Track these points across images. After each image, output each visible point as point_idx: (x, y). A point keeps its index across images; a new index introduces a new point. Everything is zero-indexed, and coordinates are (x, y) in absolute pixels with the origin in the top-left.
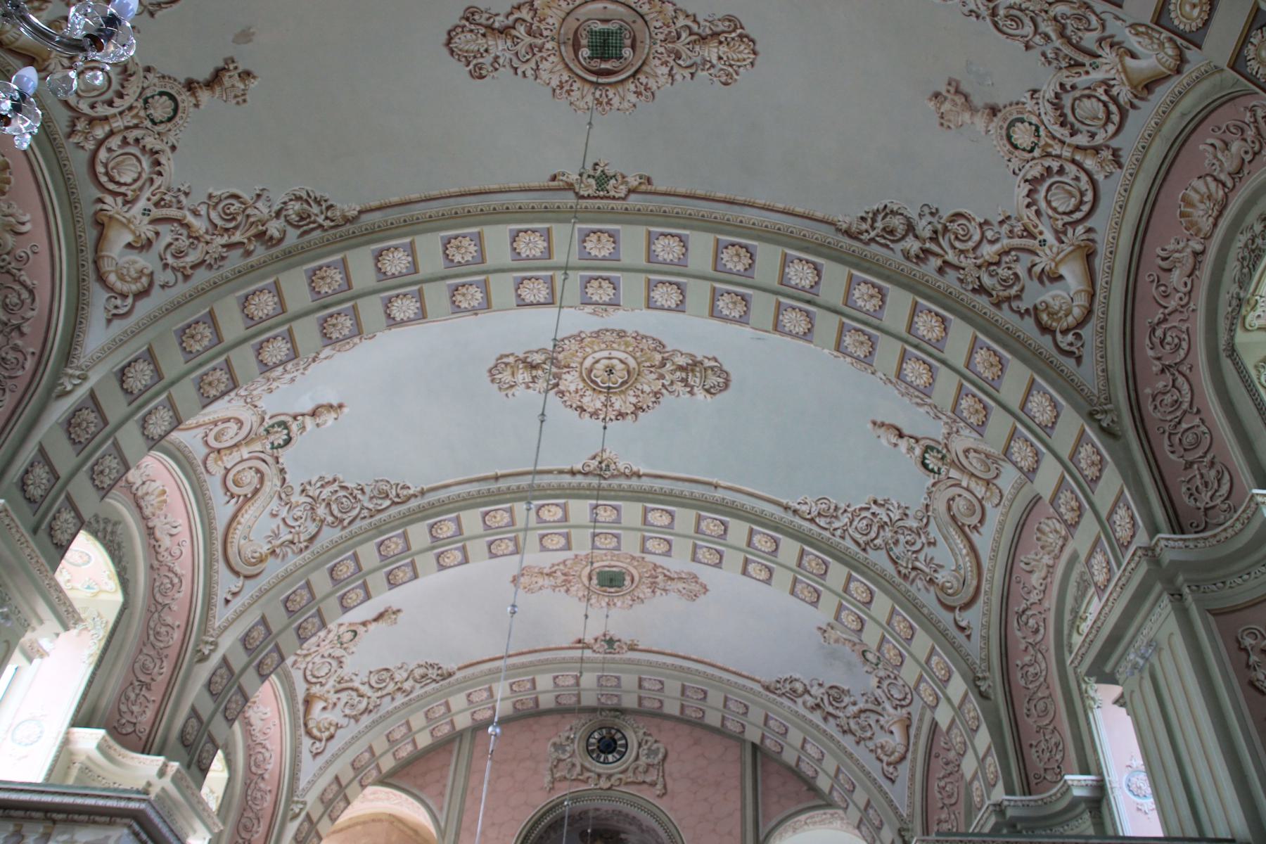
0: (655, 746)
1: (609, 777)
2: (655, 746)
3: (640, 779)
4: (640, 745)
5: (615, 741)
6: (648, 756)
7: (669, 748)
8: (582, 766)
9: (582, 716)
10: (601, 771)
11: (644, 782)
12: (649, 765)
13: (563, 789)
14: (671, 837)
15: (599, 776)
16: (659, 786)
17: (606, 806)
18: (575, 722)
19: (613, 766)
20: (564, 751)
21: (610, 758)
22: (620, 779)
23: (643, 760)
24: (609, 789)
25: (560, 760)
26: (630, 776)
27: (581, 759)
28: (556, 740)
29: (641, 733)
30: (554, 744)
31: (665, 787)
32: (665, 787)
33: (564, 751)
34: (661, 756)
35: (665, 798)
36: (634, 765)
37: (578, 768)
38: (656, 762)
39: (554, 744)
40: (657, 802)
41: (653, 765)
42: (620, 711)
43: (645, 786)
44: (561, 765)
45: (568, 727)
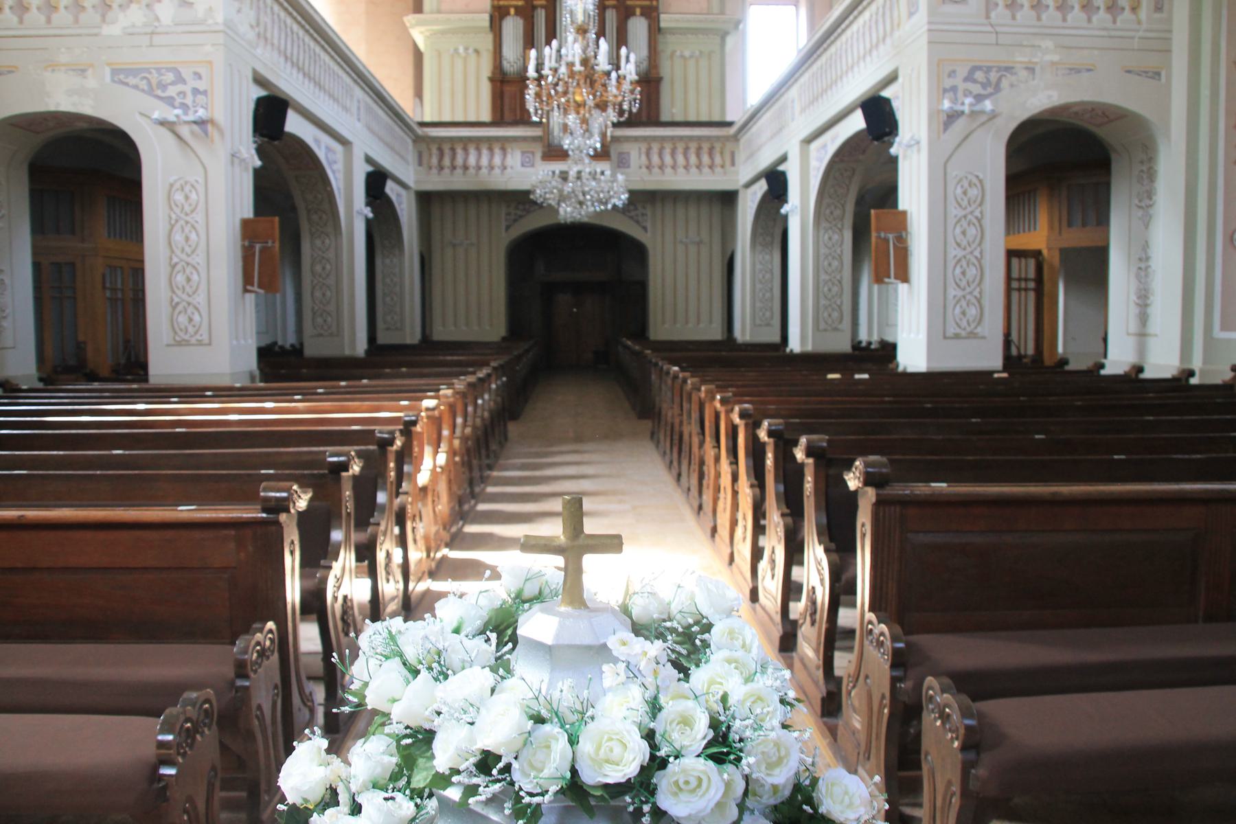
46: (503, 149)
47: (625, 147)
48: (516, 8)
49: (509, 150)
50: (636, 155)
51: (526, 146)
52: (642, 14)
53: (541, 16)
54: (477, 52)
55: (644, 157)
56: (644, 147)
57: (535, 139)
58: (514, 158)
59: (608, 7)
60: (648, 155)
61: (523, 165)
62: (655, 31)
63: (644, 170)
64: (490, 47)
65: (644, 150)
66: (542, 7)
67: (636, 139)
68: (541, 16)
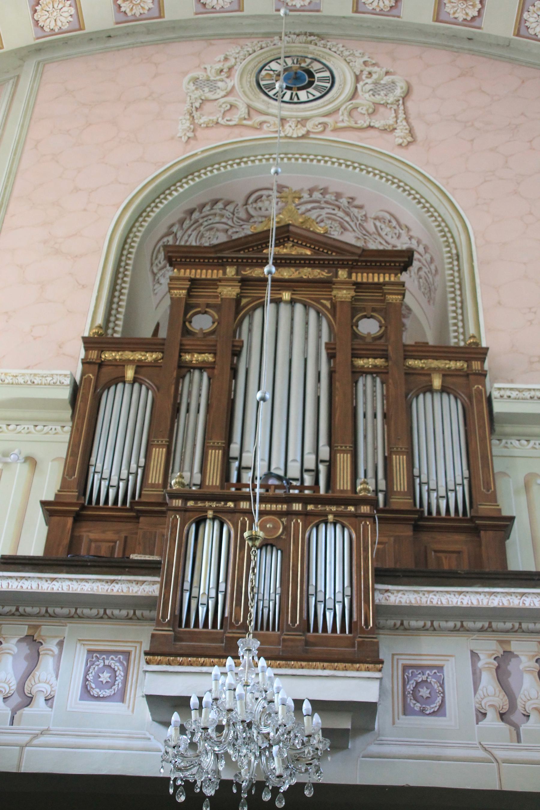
0: (387, 79)
1: (302, 121)
2: (387, 79)
3: (362, 122)
4: (357, 79)
5: (311, 75)
6: (374, 92)
7: (414, 82)
8: (249, 107)
9: (248, 42)
10: (285, 113)
11: (370, 127)
12: (376, 105)
13: (210, 142)
14: (430, 210)
15: (283, 120)
16: (401, 132)
17: (297, 182)
18: (233, 50)
19: (311, 109)
20: (214, 88)
21: (303, 95)
22: (325, 125)
23: (365, 99)
24: (303, 137)
25: (204, 101)
26: (343, 120)
27: (245, 96)
28: (200, 74)
29: (358, 64)
30: (195, 80)
31: (411, 132)
32: (411, 132)
33: (214, 88)
34: (398, 92)
35: (412, 147)
36: (349, 105)
37: (243, 111)
38: (391, 99)
39: (195, 80)
40: (398, 154)
41: (385, 105)
42: (317, 29)
43: (372, 132)
44: (208, 107)
45: (222, 57)
46: (33, 641)
47: (428, 648)
48: (140, 366)
49: (52, 645)
50: (460, 669)
51: (105, 634)
52: (444, 390)
53: (197, 390)
54: (31, 461)
55: (488, 681)
56: (487, 649)
57: (135, 609)
58: (63, 670)
59: (364, 372)
60: (501, 674)
61: (87, 693)
62: (482, 425)
63: (492, 721)
64: (62, 451)
65: (485, 660)
66: (201, 368)
67: (461, 621)
68: (197, 390)
